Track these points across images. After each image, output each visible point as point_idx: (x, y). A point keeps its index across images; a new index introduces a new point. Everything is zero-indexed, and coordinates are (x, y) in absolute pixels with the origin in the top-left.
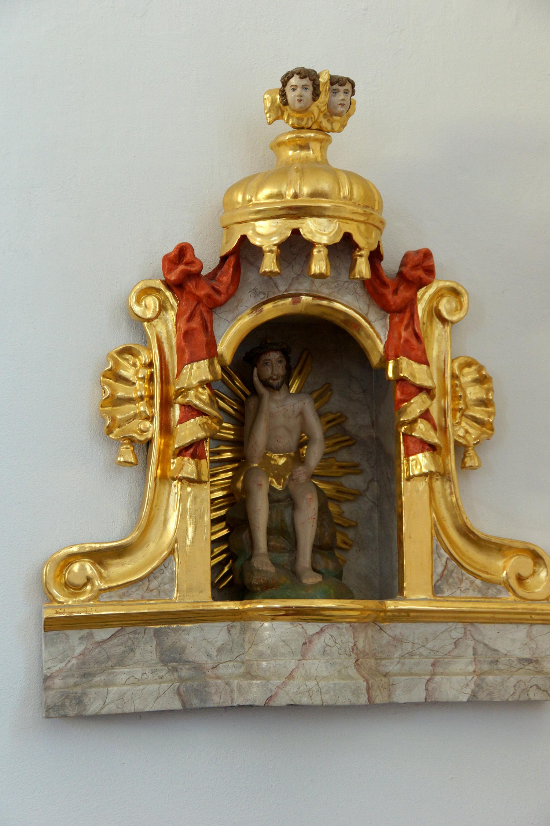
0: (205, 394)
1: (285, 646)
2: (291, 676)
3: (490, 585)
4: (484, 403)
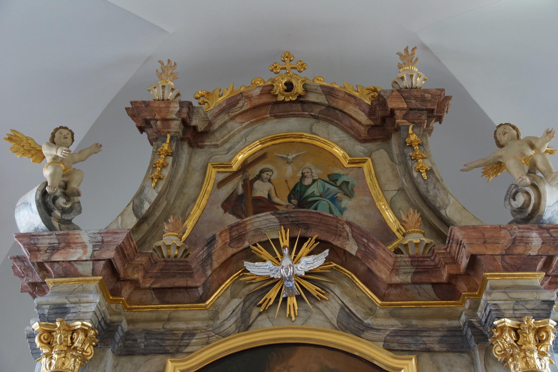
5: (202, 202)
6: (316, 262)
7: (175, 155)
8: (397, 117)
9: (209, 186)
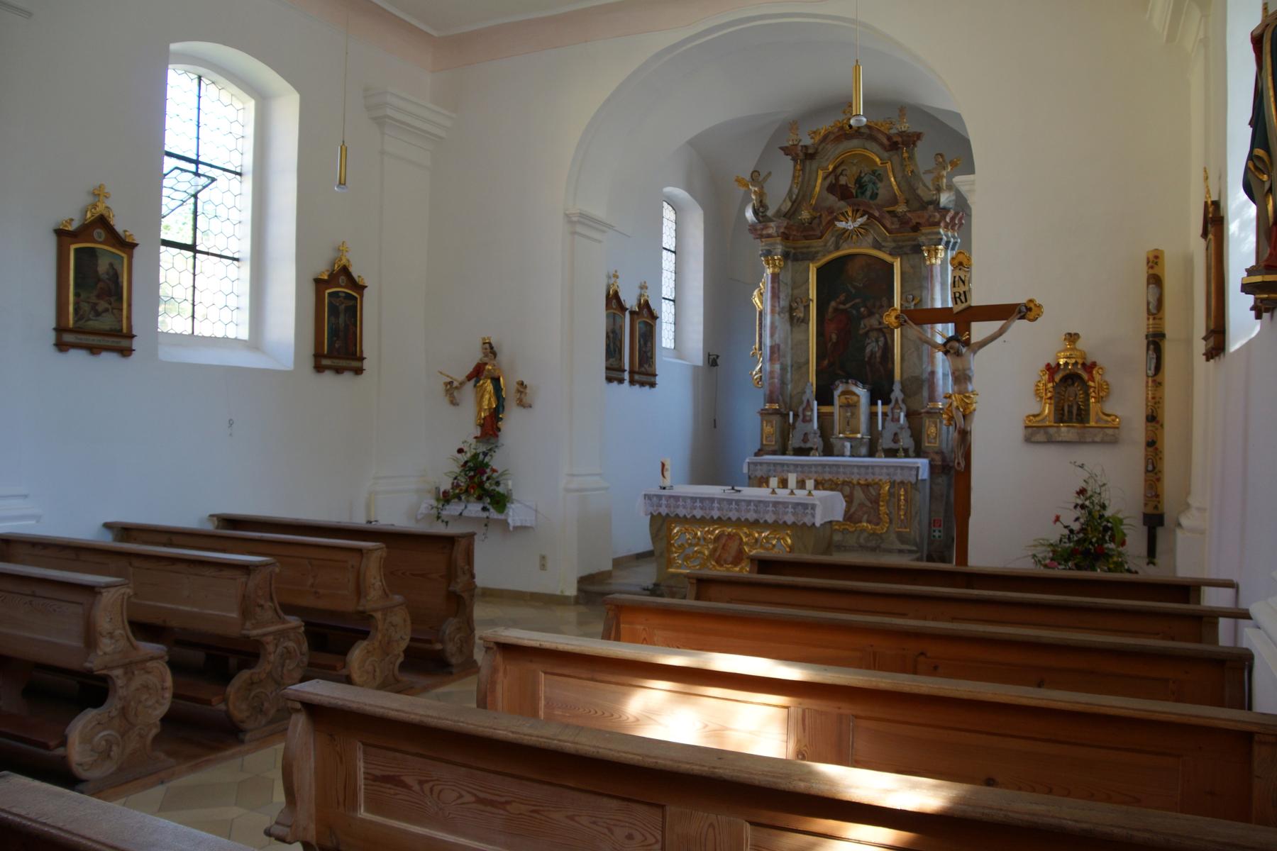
1: (1065, 431)
3: (1107, 422)
5: (817, 189)
6: (860, 221)
7: (803, 170)
8: (901, 144)
9: (819, 181)
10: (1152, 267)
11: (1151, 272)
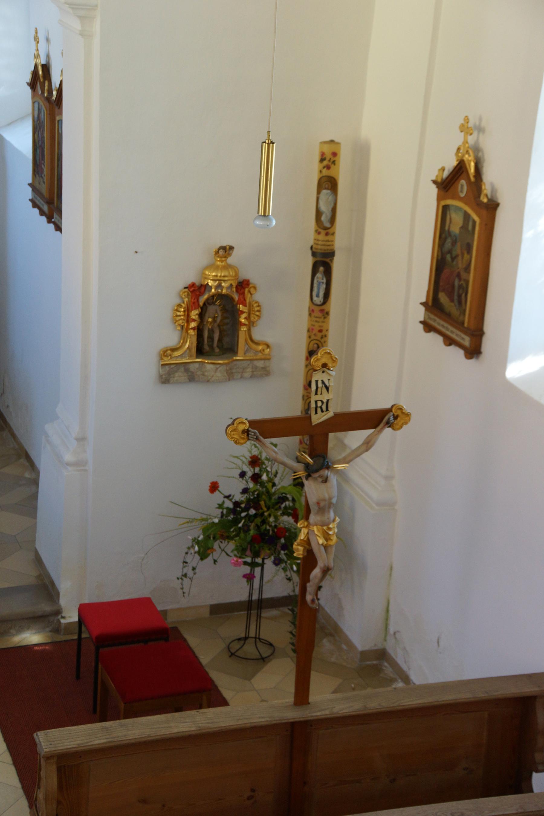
0: (197, 316)
2: (213, 376)
3: (257, 352)
4: (259, 311)
10: (328, 167)
11: (325, 172)
